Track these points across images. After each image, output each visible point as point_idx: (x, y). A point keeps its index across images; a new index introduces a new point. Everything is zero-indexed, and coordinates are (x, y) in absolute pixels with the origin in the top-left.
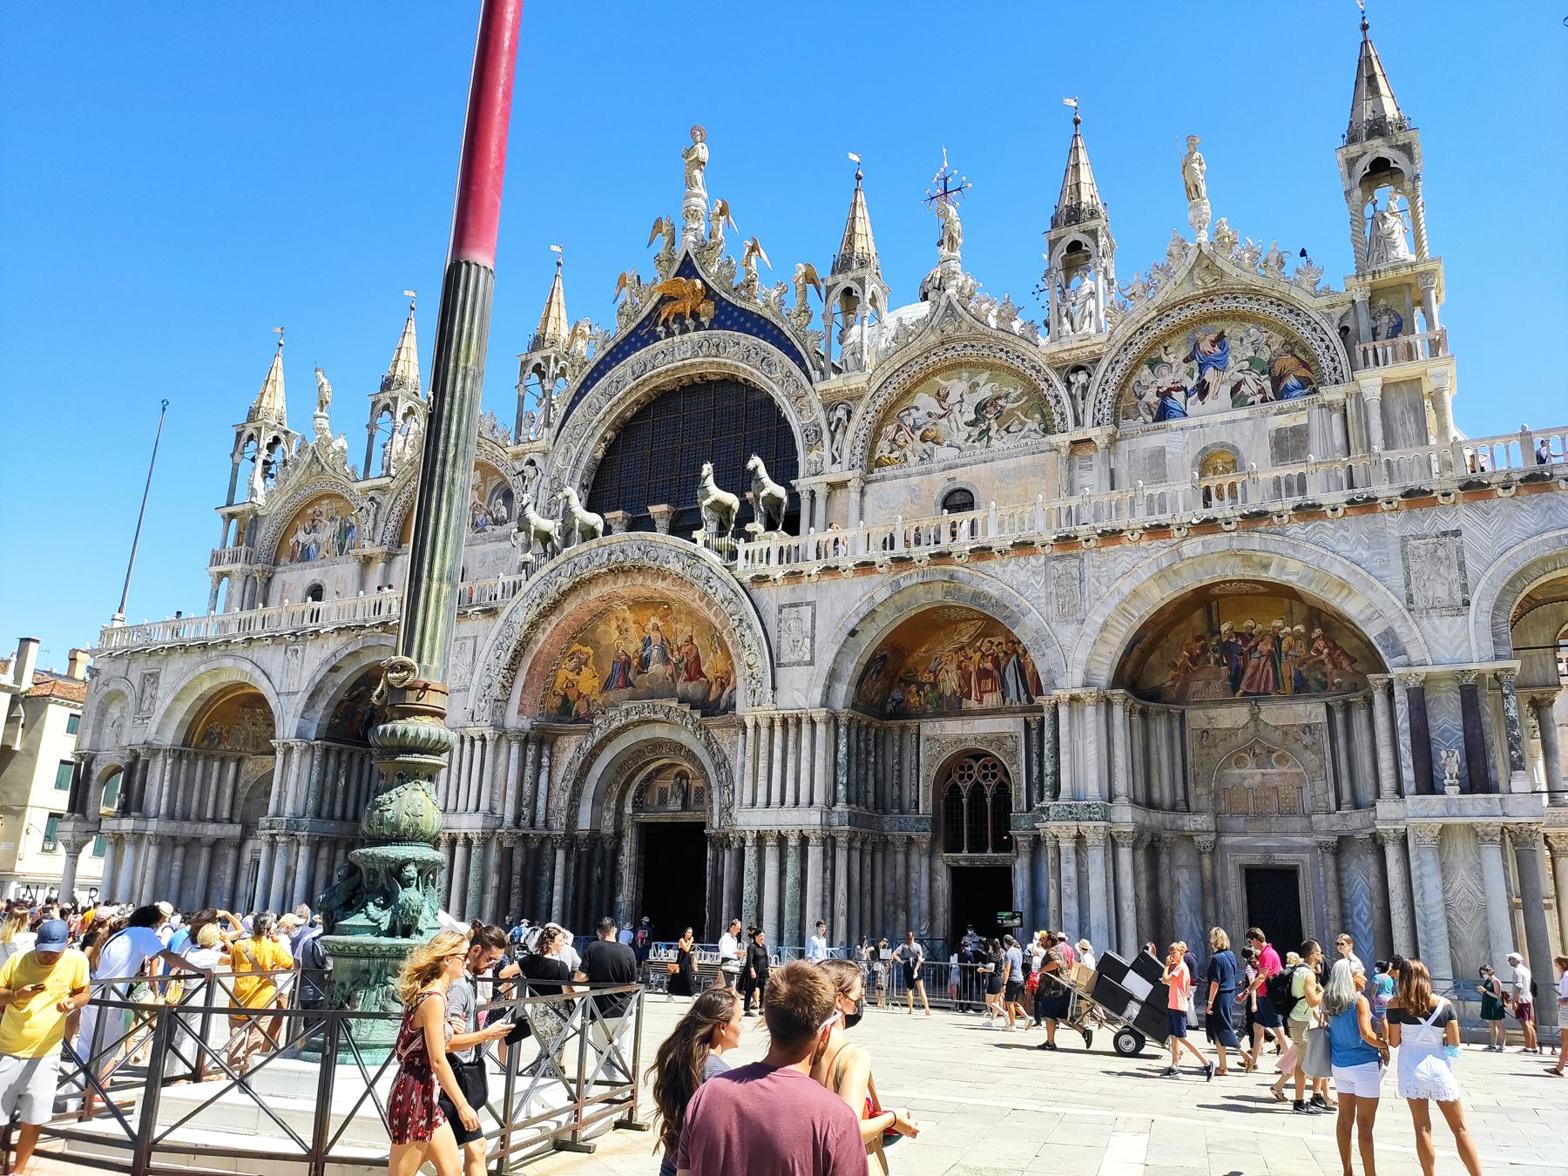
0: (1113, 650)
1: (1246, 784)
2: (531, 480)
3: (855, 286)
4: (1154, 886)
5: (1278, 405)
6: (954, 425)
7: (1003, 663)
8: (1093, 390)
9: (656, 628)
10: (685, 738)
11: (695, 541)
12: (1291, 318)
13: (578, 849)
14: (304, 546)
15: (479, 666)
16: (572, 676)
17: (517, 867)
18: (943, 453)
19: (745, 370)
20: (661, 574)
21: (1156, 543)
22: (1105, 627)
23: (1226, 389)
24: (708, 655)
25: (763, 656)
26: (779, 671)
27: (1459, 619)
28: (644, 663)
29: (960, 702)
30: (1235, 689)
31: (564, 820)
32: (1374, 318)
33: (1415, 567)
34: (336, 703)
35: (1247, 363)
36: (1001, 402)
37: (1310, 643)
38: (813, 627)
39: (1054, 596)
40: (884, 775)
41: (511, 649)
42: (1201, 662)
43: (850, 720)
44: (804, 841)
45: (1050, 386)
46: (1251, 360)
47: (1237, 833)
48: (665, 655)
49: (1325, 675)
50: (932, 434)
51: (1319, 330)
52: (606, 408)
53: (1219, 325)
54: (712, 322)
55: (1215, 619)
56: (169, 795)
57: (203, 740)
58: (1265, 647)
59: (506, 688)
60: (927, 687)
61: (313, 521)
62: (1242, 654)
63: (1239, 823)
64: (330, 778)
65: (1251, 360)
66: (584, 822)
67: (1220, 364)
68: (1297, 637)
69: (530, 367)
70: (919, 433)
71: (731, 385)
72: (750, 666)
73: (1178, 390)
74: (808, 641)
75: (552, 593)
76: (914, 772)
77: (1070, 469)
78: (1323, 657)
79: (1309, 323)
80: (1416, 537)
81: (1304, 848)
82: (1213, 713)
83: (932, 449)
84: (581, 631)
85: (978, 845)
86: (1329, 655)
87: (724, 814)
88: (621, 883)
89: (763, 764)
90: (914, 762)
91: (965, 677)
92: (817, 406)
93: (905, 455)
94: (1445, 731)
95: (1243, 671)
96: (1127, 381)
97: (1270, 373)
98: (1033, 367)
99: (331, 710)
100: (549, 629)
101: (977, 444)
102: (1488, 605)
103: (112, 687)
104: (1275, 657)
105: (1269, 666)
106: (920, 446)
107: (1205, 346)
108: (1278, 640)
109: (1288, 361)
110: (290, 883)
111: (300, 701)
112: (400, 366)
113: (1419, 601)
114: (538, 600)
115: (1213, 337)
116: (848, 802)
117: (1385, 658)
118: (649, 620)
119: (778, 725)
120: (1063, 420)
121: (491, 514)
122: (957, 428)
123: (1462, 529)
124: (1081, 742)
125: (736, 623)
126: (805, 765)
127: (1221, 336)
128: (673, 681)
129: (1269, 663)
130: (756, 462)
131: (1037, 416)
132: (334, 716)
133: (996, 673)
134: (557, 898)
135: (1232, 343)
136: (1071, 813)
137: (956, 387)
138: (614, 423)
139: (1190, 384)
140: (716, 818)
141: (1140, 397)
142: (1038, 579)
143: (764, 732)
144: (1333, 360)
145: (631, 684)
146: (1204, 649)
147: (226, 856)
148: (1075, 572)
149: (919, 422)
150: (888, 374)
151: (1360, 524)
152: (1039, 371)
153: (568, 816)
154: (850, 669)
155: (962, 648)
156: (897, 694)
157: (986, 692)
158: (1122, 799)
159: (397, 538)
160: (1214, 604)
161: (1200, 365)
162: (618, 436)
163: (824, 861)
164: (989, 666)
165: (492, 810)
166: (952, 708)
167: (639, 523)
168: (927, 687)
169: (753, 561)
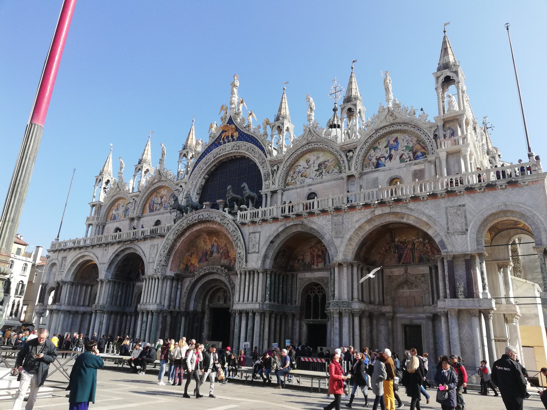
0: (353, 247)
1: (404, 295)
2: (181, 192)
3: (281, 125)
4: (371, 331)
5: (414, 161)
6: (311, 171)
7: (325, 252)
8: (355, 158)
9: (215, 241)
10: (223, 279)
12: (418, 132)
13: (189, 316)
15: (158, 254)
16: (189, 258)
18: (308, 181)
19: (247, 154)
20: (214, 222)
21: (367, 210)
22: (350, 239)
23: (398, 157)
25: (243, 250)
26: (249, 256)
27: (464, 236)
28: (212, 253)
29: (311, 266)
30: (400, 261)
31: (184, 307)
32: (445, 131)
33: (450, 218)
35: (405, 148)
36: (326, 163)
37: (424, 245)
38: (259, 240)
39: (334, 229)
40: (286, 291)
43: (271, 272)
44: (254, 314)
45: (341, 157)
46: (406, 147)
47: (401, 313)
48: (218, 250)
49: (429, 256)
50: (304, 174)
51: (427, 135)
53: (396, 135)
54: (238, 138)
55: (393, 236)
56: (68, 297)
57: (80, 279)
58: (410, 246)
59: (167, 261)
60: (301, 261)
61: (117, 207)
62: (402, 249)
63: (402, 309)
64: (115, 292)
65: (406, 147)
66: (191, 308)
67: (396, 148)
68: (420, 243)
69: (182, 155)
70: (300, 174)
71: (243, 158)
72: (239, 254)
73: (383, 157)
74: (257, 245)
75: (181, 229)
76: (295, 290)
77: (347, 185)
78: (428, 250)
79: (424, 133)
80: (451, 207)
81: (423, 318)
82: (393, 270)
83: (304, 179)
84: (192, 242)
85: (316, 317)
86: (431, 249)
88: (204, 329)
89: (242, 287)
90: (296, 287)
91: (313, 257)
92: (269, 165)
93: (296, 182)
94: (461, 276)
95: (403, 255)
96: (366, 155)
97: (412, 151)
98: (336, 151)
100: (181, 242)
101: (318, 177)
102: (475, 231)
103: (53, 262)
104: (413, 250)
105: (411, 253)
106: (300, 178)
107: (392, 142)
108: (414, 244)
109: (418, 147)
110: (101, 327)
111: (106, 266)
112: (145, 156)
113: (451, 231)
114: (177, 232)
115: (394, 139)
116: (270, 300)
117: (441, 250)
118: (213, 238)
119: (247, 273)
120: (345, 168)
121: (169, 204)
122: (312, 172)
123: (465, 204)
124: (342, 280)
125: (236, 239)
126: (255, 288)
127: (397, 138)
128: (220, 259)
129: (411, 252)
130: (245, 184)
131: (338, 167)
132: (117, 271)
133: (323, 256)
135: (400, 141)
136: (337, 304)
137: (312, 157)
138: (207, 172)
139: (387, 155)
141: (371, 160)
142: (329, 223)
143: (243, 276)
144: (432, 146)
145: (208, 260)
146: (390, 247)
147: (86, 318)
148: (341, 220)
149: (301, 170)
150: (290, 154)
151: (431, 203)
152: (338, 152)
153: (186, 305)
154: (271, 254)
155: (312, 247)
156: (291, 263)
157: (319, 262)
158: (356, 300)
159: (141, 212)
160: (393, 231)
161: (390, 149)
162: (209, 178)
164: (320, 253)
165: (160, 303)
166: (308, 268)
167: (215, 206)
168: (301, 261)
169: (242, 218)
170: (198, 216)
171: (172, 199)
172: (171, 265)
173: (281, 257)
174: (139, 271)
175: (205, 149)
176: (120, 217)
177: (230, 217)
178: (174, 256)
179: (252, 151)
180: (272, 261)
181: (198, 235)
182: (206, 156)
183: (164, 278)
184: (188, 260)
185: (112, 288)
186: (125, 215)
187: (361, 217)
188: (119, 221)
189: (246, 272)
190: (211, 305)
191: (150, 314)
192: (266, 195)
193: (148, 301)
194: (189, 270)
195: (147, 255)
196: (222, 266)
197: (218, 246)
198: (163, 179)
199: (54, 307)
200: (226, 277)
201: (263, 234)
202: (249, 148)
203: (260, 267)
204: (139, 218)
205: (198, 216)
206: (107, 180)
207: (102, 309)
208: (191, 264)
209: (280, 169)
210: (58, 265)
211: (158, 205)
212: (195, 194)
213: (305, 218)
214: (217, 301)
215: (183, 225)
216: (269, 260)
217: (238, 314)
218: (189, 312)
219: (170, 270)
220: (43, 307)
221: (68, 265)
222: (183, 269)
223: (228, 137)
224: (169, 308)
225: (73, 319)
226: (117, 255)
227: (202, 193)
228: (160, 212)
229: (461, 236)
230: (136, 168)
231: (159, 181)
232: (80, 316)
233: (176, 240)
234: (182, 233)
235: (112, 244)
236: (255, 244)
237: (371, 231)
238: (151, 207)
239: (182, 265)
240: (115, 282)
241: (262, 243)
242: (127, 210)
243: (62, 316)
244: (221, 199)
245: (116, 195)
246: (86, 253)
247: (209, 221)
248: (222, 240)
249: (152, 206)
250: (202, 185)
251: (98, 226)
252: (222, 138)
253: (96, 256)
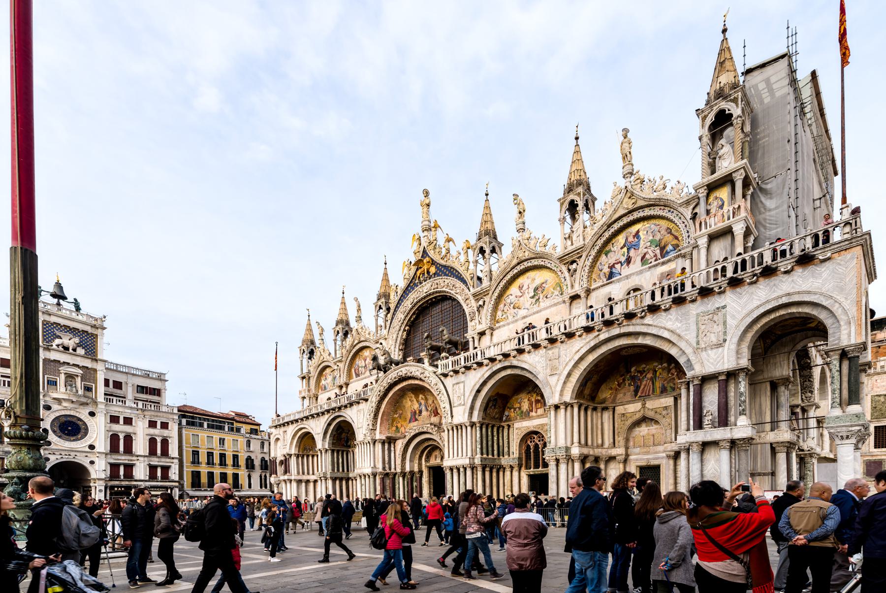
26: (454, 409)
27: (720, 349)
29: (529, 414)
38: (464, 391)
42: (623, 385)
49: (674, 384)
58: (649, 375)
60: (517, 409)
62: (639, 380)
74: (462, 397)
91: (531, 404)
95: (640, 387)
104: (653, 380)
133: (542, 401)
146: (624, 380)
156: (506, 413)
164: (539, 398)
168: (517, 409)
173: (493, 407)
177: (432, 369)
181: (403, 393)
187: (582, 345)
201: (467, 383)
212: (397, 350)
213: (514, 357)
229: (716, 349)
232: (304, 484)
237: (595, 362)
241: (467, 394)
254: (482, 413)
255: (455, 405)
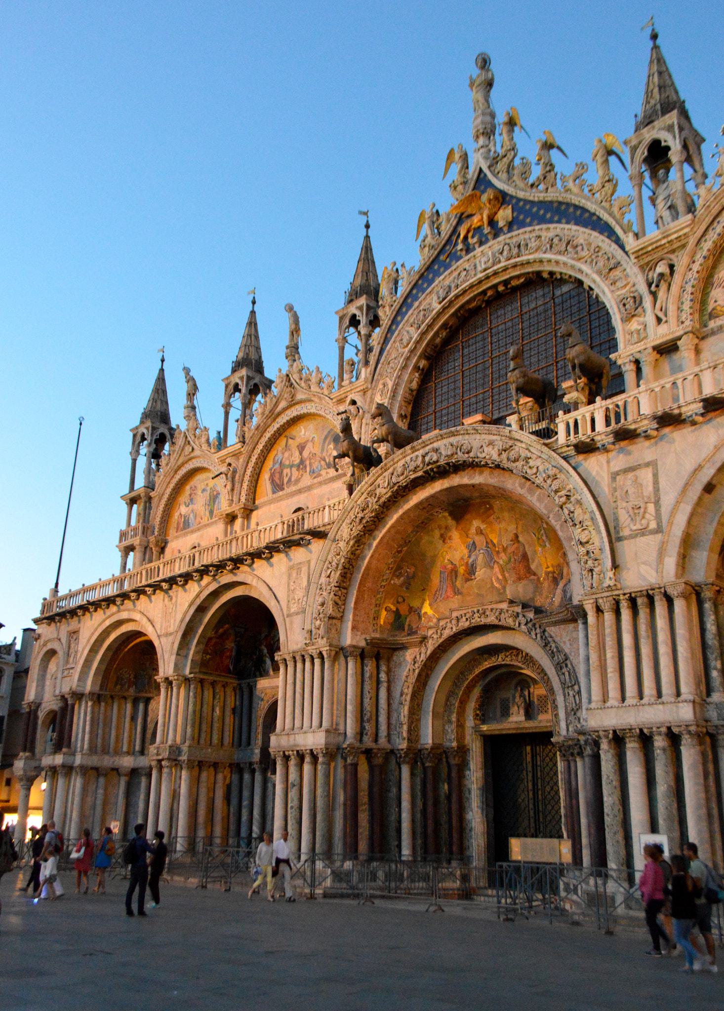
11: (510, 425)
13: (423, 764)
14: (185, 517)
15: (313, 587)
17: (364, 784)
24: (535, 552)
26: (621, 546)
28: (471, 570)
34: (205, 641)
41: (340, 567)
52: (415, 336)
56: (91, 732)
59: (340, 602)
66: (427, 739)
75: (373, 503)
87: (572, 718)
99: (202, 646)
100: (375, 544)
103: (49, 646)
110: (175, 805)
114: (360, 515)
118: (471, 523)
121: (324, 460)
125: (563, 499)
126: (664, 650)
132: (205, 652)
134: (406, 816)
140: (563, 725)
143: (609, 617)
147: (140, 783)
163: (705, 764)
170: (424, 457)
171: (332, 446)
172: (355, 615)
174: (261, 651)
175: (413, 283)
176: (198, 519)
178: (359, 588)
179: (568, 243)
180: (715, 556)
182: (416, 304)
183: (337, 653)
184: (400, 600)
185: (195, 697)
186: (211, 512)
188: (199, 529)
189: (617, 603)
190: (484, 728)
191: (308, 759)
192: (637, 362)
193: (298, 724)
194: (406, 628)
195: (282, 594)
196: (511, 602)
197: (489, 544)
198: (300, 396)
199: (59, 759)
200: (533, 633)
202: (556, 240)
203: (673, 579)
204: (248, 511)
205: (424, 457)
206: (158, 433)
207: (174, 757)
208: (411, 609)
209: (679, 269)
210: (61, 653)
211: (294, 469)
214: (498, 714)
215: (378, 491)
216: (705, 554)
217: (610, 742)
218: (420, 751)
219: (354, 628)
220: (33, 764)
221: (83, 650)
222: (389, 627)
223: (479, 229)
224: (361, 741)
225: (106, 790)
226: (201, 609)
227: (412, 415)
228: (301, 485)
230: (227, 386)
231: (292, 404)
232: (123, 781)
233: (360, 541)
234: (376, 516)
235: (187, 577)
236: (642, 505)
238: (276, 479)
239: (384, 614)
240: (202, 681)
242: (214, 497)
243: (77, 782)
244: (476, 411)
245: (183, 464)
246: (124, 615)
247: (457, 468)
248: (503, 525)
249: (277, 475)
250: (412, 390)
251: (148, 549)
252: (462, 237)
253: (148, 618)
254: (717, 556)
255: (621, 534)
